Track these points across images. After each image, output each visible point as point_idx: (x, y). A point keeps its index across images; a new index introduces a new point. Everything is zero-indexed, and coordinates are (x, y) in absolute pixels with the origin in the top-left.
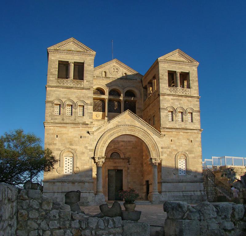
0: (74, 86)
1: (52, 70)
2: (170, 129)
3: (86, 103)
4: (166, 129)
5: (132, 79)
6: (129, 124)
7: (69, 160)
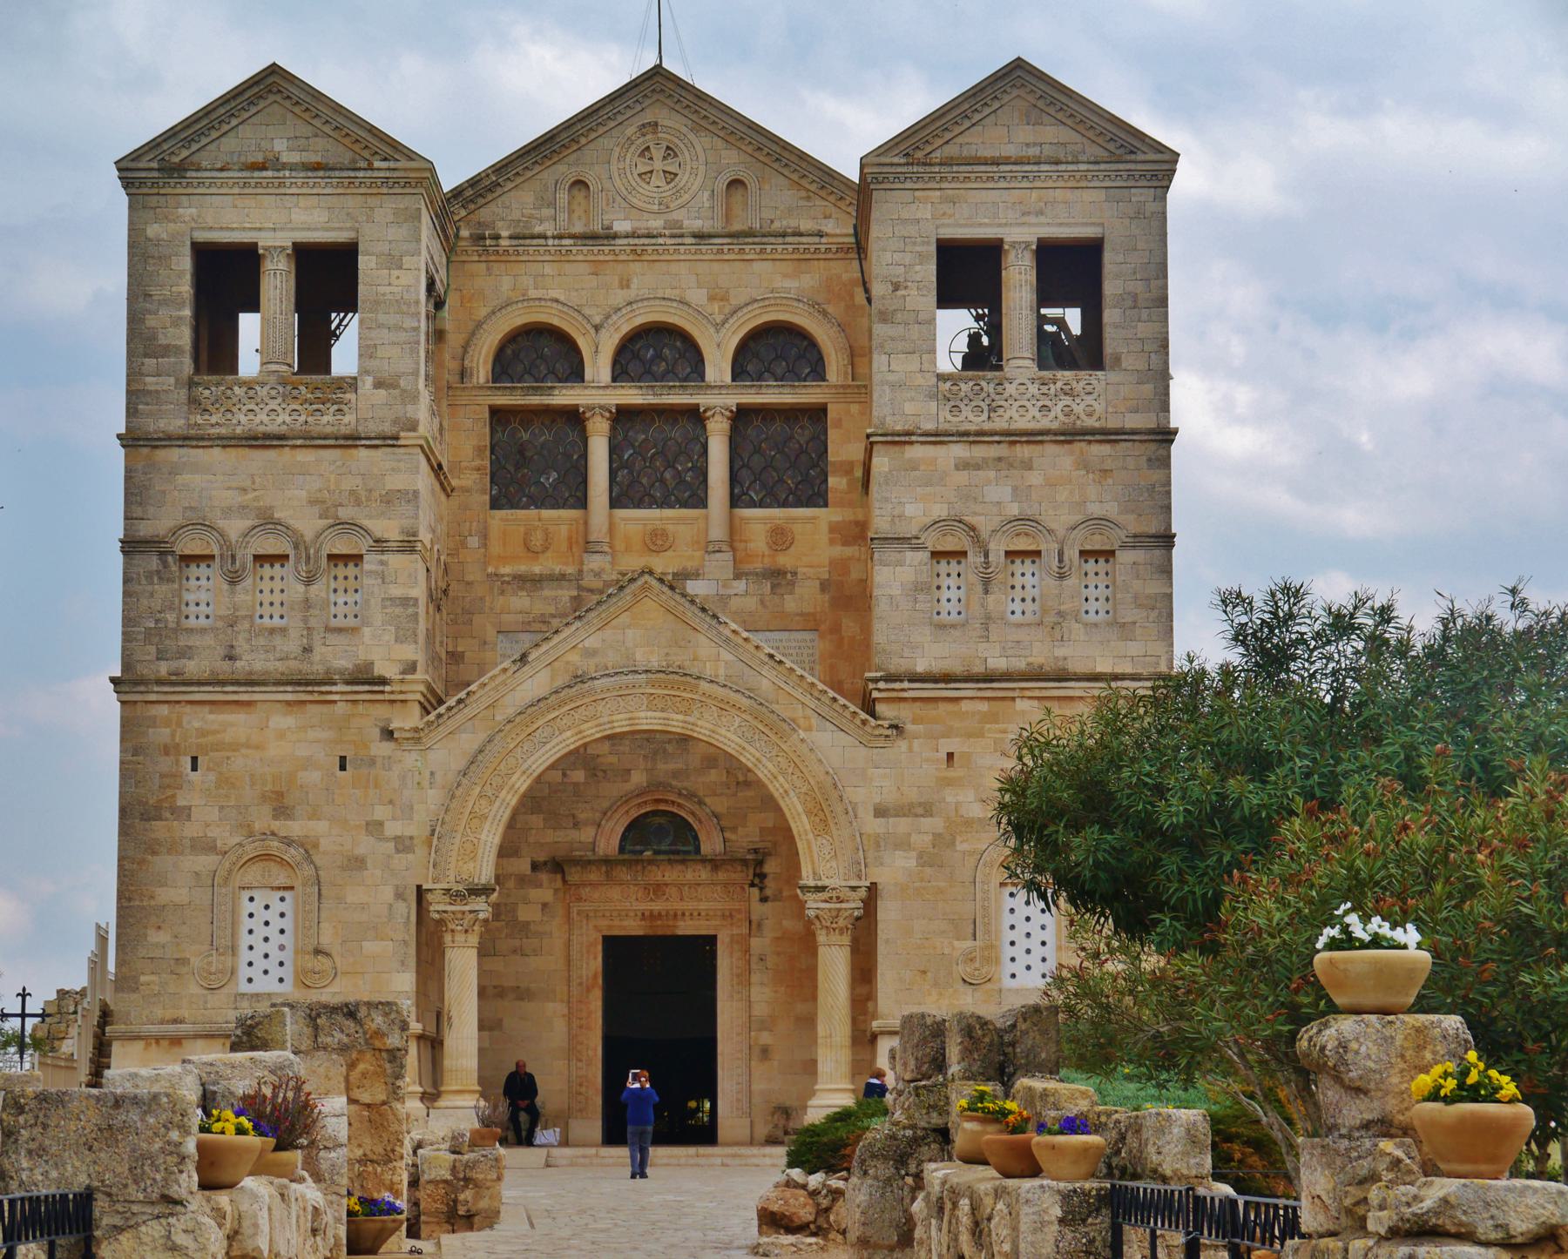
1: (151, 321)
2: (936, 681)
3: (378, 535)
4: (906, 685)
5: (784, 235)
6: (655, 665)
7: (267, 907)
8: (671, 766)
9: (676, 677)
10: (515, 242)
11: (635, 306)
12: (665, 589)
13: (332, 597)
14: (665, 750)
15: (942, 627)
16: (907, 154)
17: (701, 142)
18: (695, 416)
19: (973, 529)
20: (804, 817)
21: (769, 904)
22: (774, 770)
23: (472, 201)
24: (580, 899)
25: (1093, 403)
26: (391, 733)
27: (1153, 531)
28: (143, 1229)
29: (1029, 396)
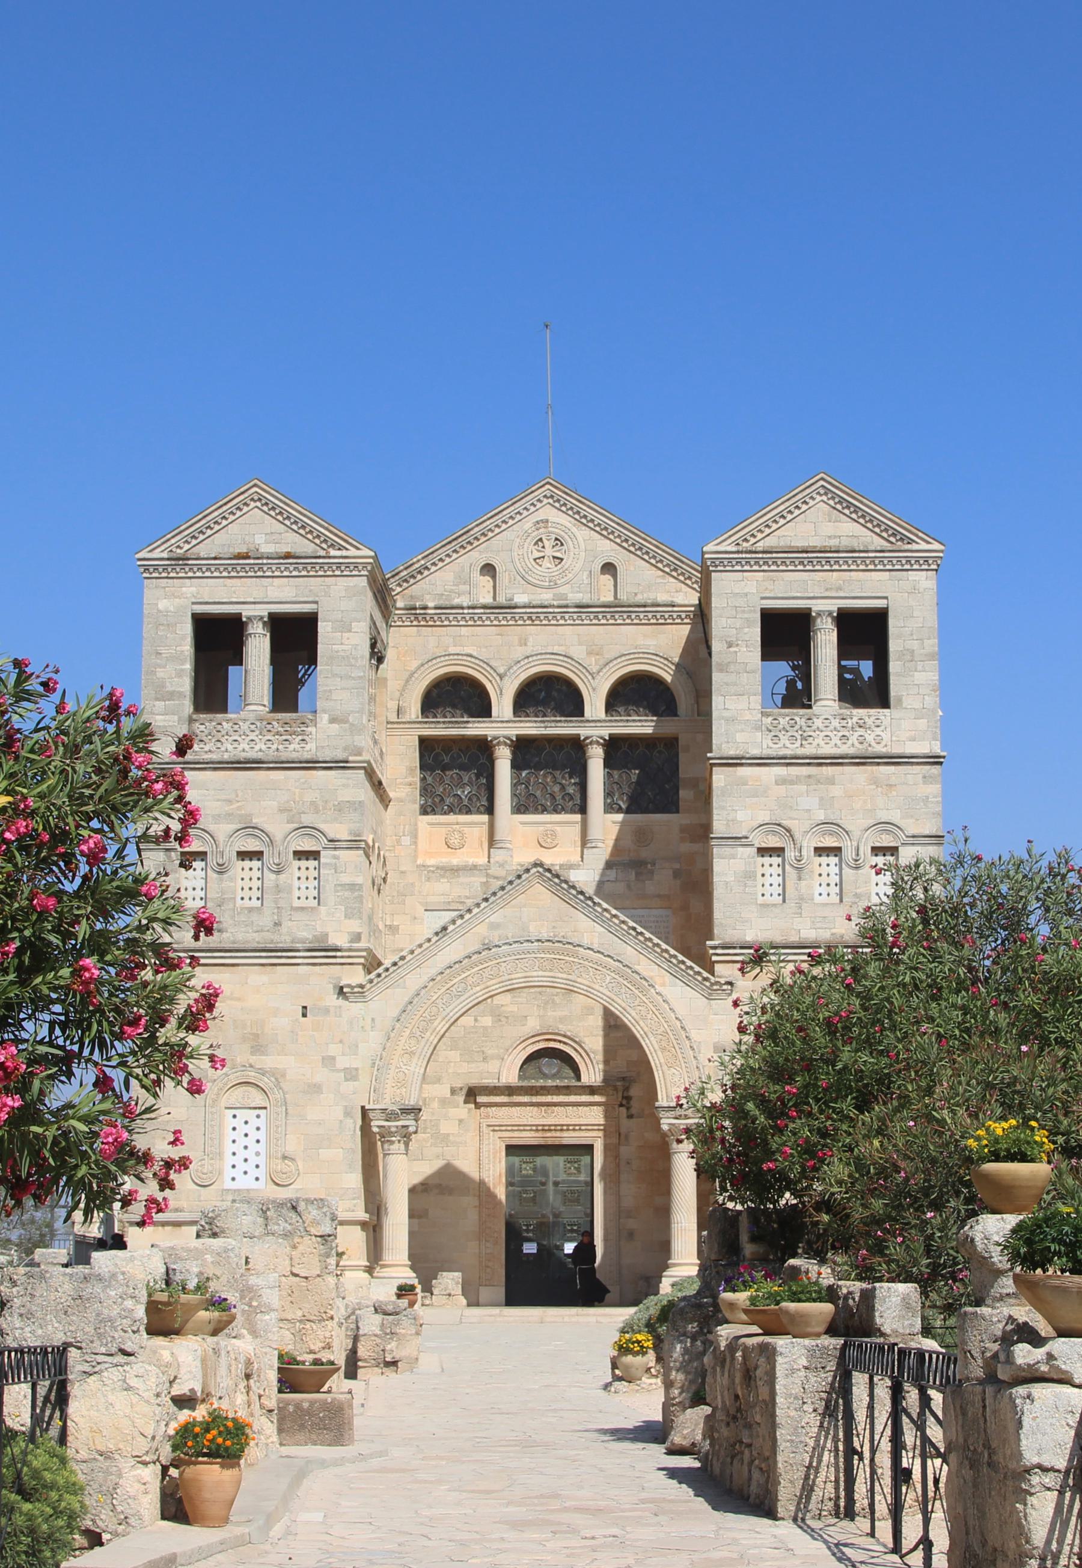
0: (271, 755)
1: (161, 673)
3: (331, 836)
5: (645, 606)
6: (545, 936)
7: (246, 1122)
8: (559, 1013)
11: (531, 659)
13: (296, 883)
14: (553, 1001)
15: (764, 906)
16: (738, 544)
17: (583, 534)
18: (576, 747)
19: (788, 830)
20: (659, 1053)
21: (634, 1120)
22: (637, 1017)
23: (406, 581)
24: (488, 1117)
25: (881, 733)
26: (342, 988)
27: (927, 832)
28: (105, 1374)
29: (832, 728)
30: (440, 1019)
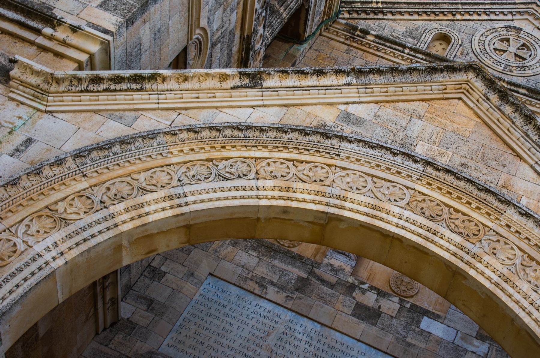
9: (470, 188)
10: (377, 40)
12: (494, 98)
23: (357, 12)
30: (162, 193)
